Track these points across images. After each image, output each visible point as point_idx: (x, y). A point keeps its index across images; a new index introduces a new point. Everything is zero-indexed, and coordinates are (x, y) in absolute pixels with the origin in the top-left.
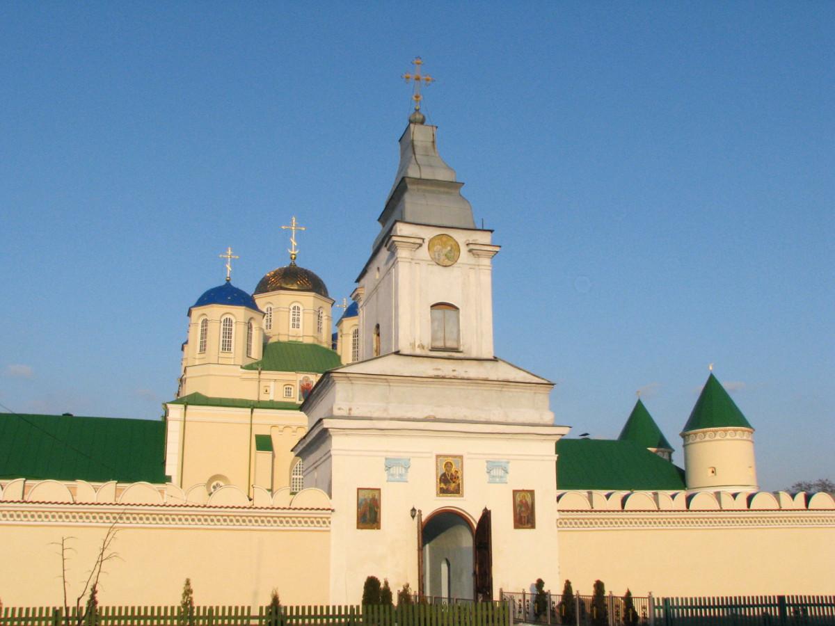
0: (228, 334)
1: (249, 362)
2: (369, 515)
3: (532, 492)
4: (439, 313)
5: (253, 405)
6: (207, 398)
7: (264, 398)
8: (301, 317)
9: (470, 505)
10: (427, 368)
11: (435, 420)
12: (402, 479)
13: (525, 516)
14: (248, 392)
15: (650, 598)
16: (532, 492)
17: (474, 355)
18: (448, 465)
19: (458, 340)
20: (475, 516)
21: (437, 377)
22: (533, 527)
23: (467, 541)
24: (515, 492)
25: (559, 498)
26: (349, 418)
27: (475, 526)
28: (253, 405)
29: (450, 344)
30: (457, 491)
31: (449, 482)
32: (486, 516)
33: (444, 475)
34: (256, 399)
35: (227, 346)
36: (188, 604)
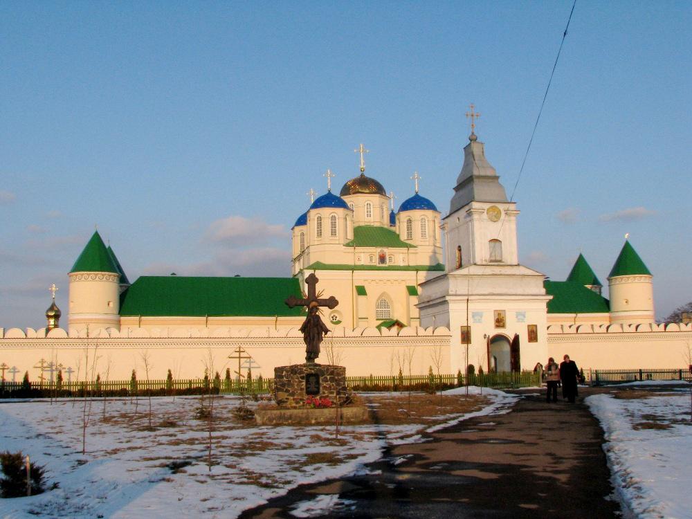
0: (333, 225)
1: (348, 241)
2: (466, 337)
3: (536, 326)
4: (493, 244)
5: (353, 268)
6: (324, 265)
7: (358, 263)
8: (372, 210)
9: (509, 332)
10: (488, 271)
11: (494, 295)
12: (480, 321)
13: (533, 336)
14: (348, 260)
15: (591, 370)
16: (536, 326)
17: (509, 263)
18: (499, 314)
19: (501, 257)
20: (511, 338)
21: (493, 275)
22: (537, 341)
23: (507, 348)
24: (529, 326)
25: (548, 328)
26: (456, 295)
27: (511, 341)
28: (353, 268)
29: (498, 258)
30: (503, 326)
31: (500, 322)
32: (517, 338)
33: (498, 319)
34: (353, 264)
35: (333, 233)
36: (431, 374)
